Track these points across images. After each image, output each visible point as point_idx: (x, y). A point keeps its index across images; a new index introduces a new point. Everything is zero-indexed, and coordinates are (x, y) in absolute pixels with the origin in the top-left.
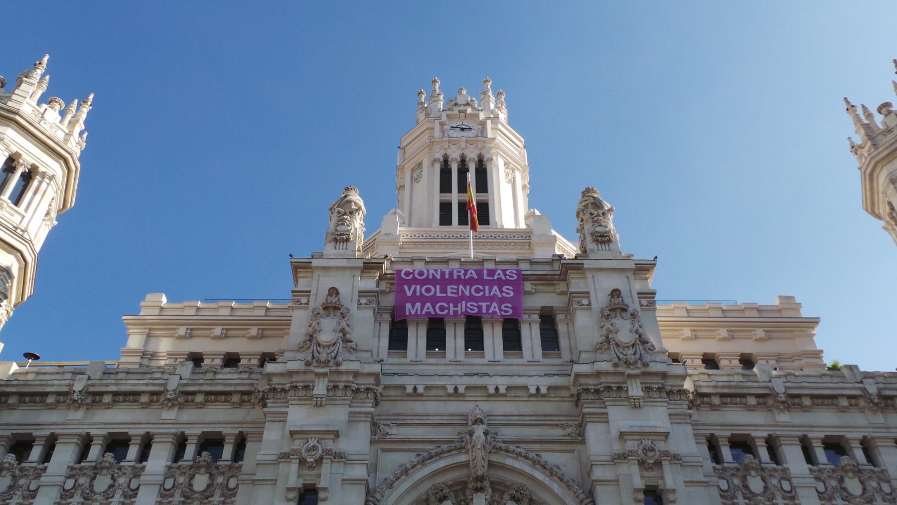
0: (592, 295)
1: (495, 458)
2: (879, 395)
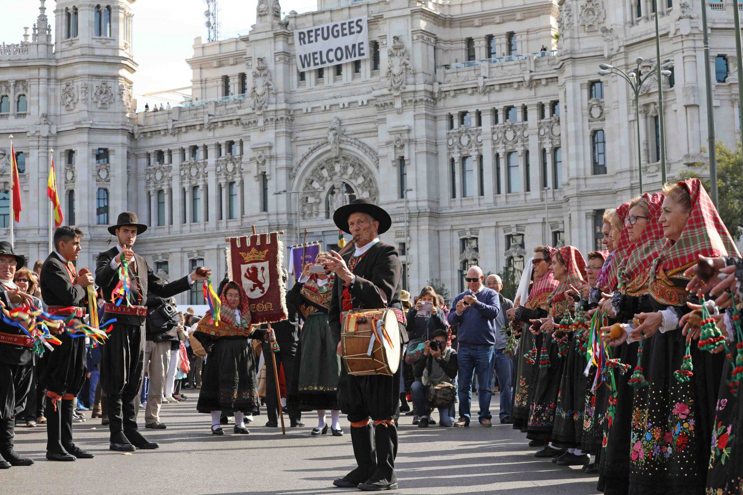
0: (388, 37)
1: (342, 146)
2: (531, 81)
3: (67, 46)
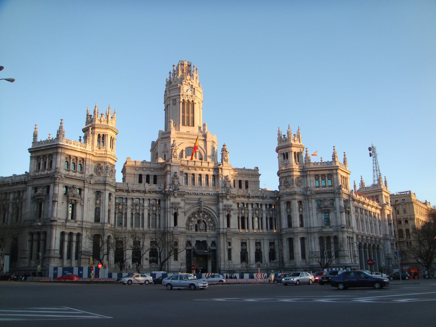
1: (204, 207)
3: (99, 149)
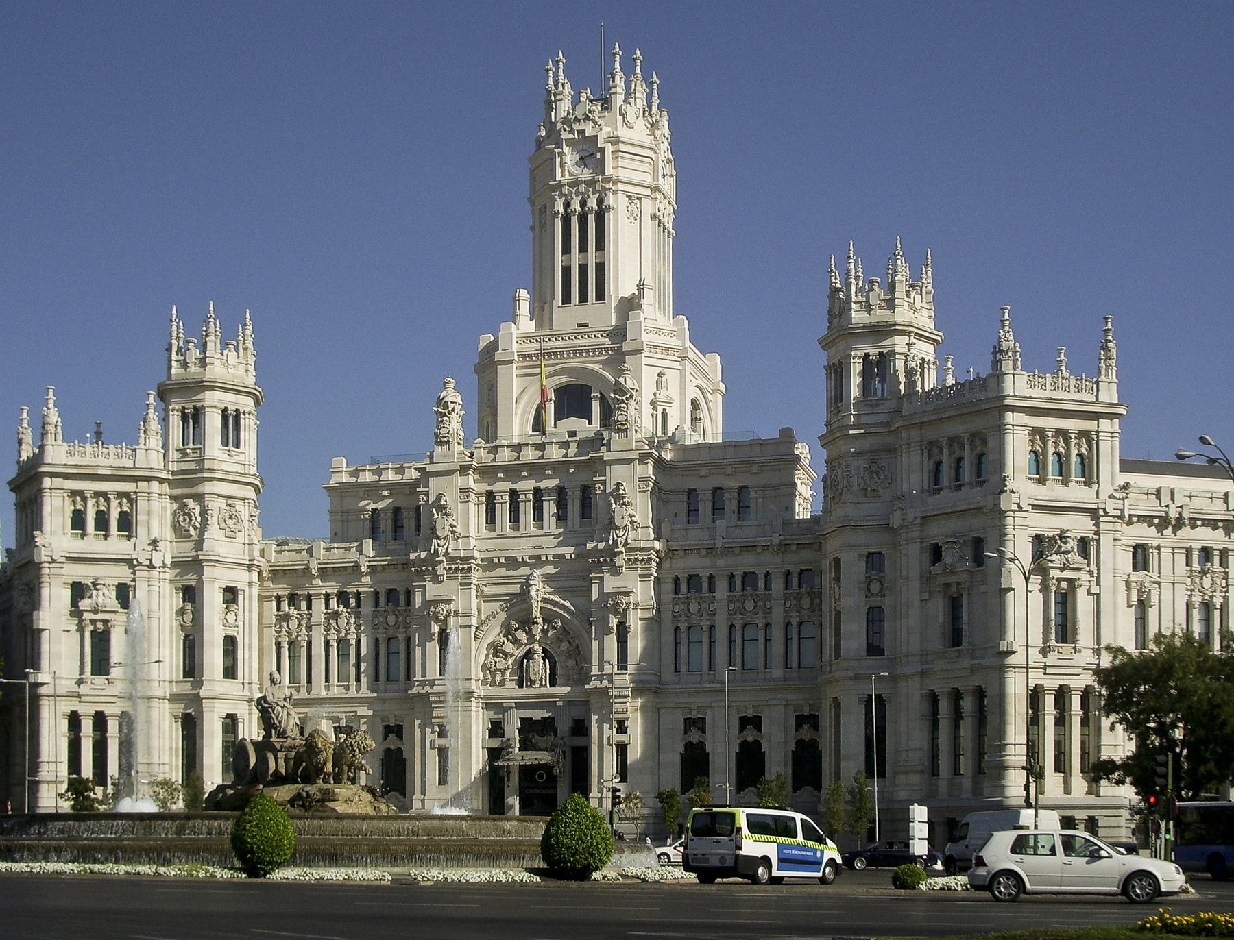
2: (780, 545)
